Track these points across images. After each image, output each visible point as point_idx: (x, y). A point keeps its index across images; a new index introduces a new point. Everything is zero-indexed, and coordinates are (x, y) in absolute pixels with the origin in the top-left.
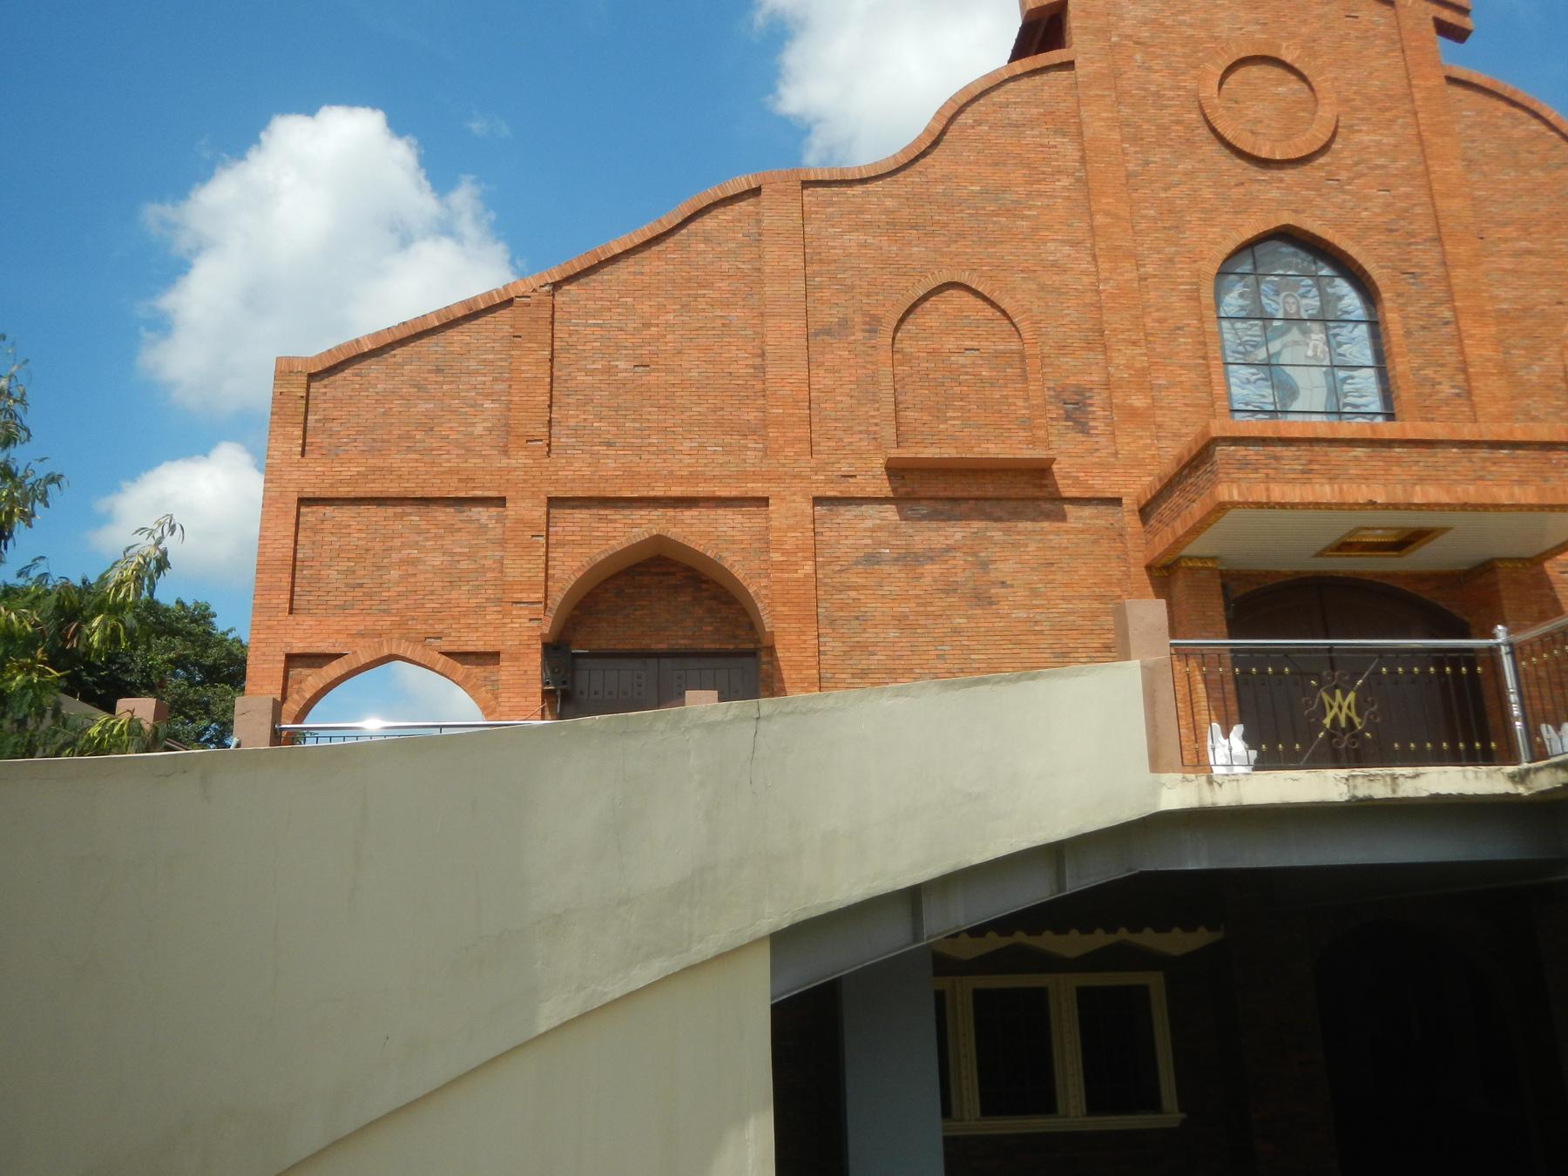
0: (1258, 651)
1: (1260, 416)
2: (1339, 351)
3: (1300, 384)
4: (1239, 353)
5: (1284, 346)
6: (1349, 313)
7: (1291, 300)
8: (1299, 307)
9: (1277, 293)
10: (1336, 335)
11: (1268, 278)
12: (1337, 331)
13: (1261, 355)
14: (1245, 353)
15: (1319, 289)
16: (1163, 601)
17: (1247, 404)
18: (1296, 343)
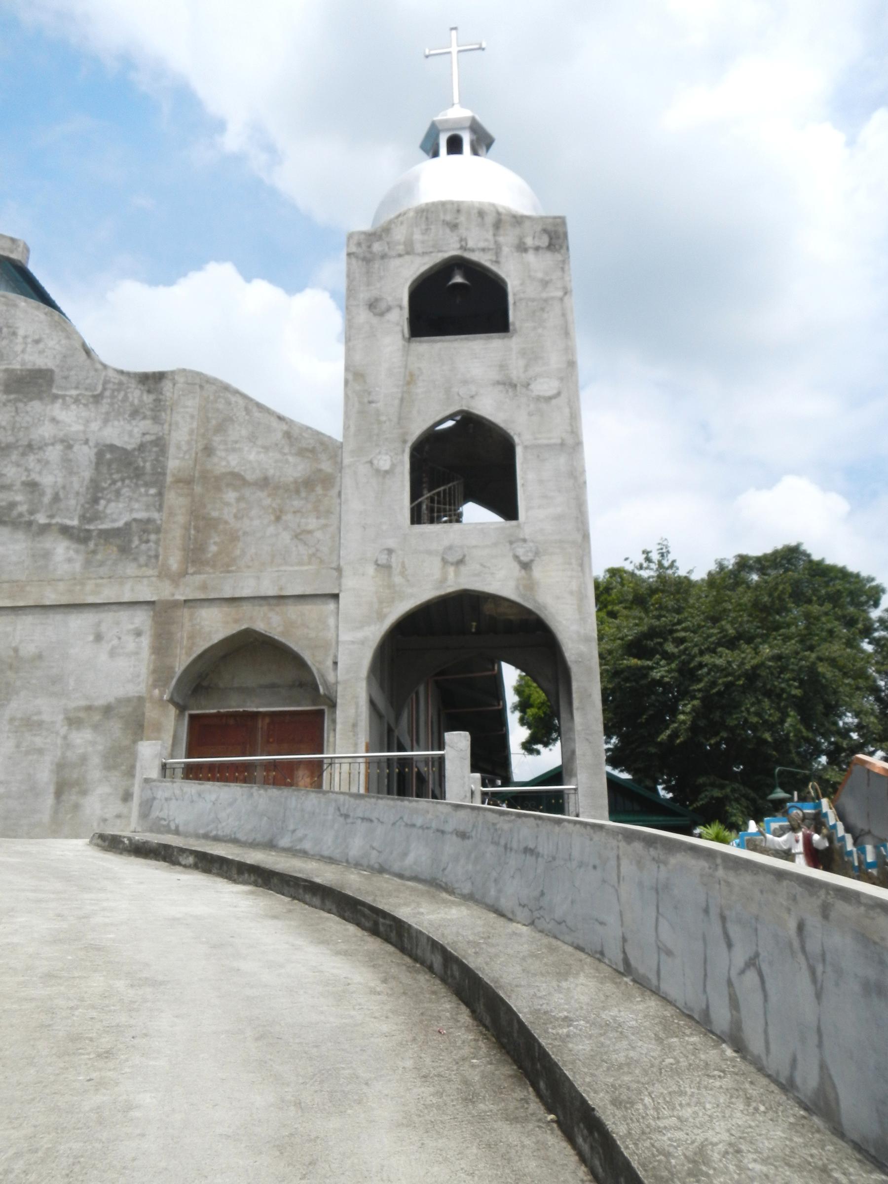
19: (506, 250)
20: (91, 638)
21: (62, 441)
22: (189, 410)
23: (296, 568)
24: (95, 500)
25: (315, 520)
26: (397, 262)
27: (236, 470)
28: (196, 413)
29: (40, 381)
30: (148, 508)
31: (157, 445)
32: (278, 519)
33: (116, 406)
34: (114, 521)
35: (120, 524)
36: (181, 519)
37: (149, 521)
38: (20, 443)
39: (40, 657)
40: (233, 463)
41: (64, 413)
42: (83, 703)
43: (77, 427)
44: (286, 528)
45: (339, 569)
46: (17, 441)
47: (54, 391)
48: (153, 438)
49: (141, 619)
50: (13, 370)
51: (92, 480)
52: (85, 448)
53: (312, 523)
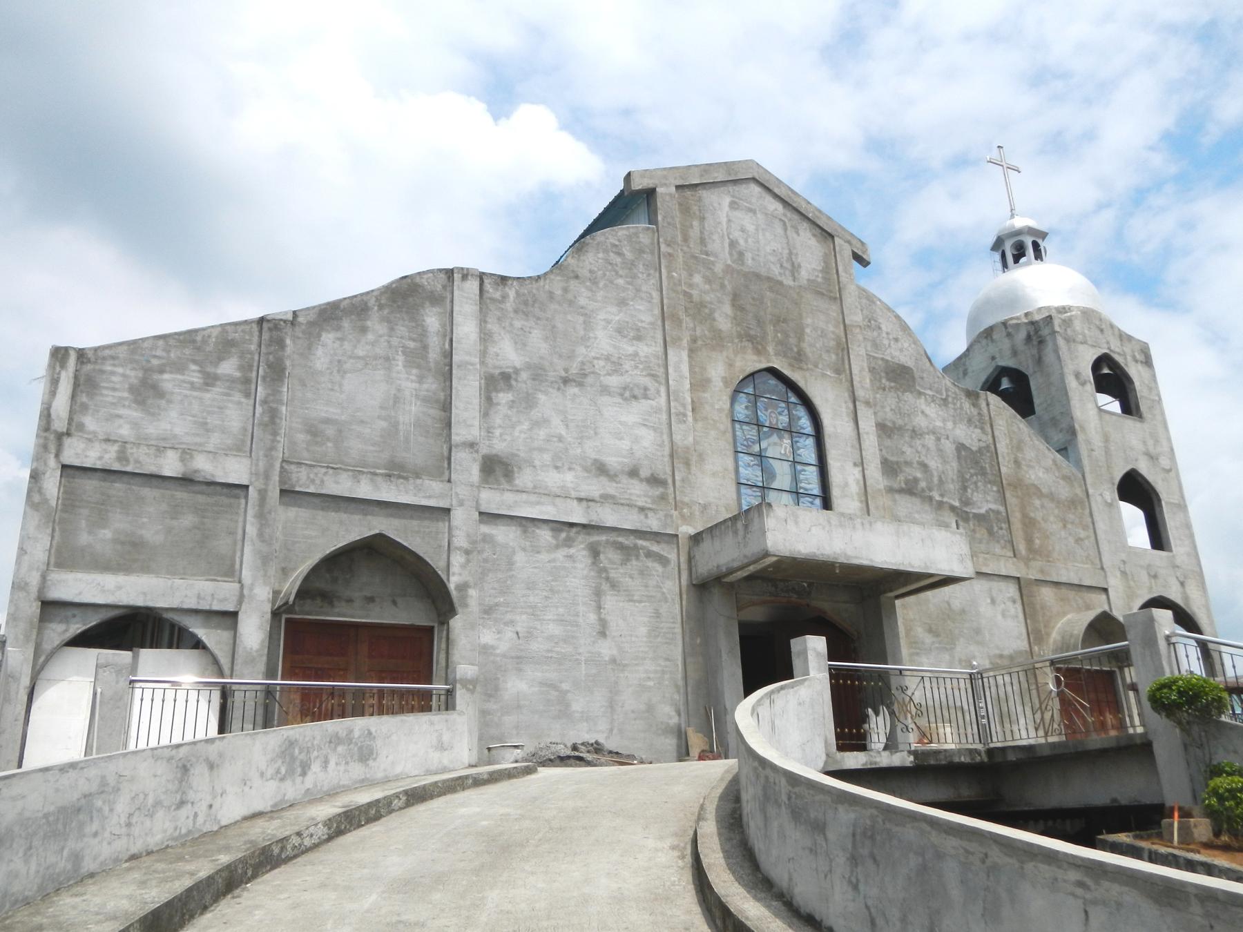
0: (851, 670)
1: (755, 489)
2: (799, 452)
3: (777, 472)
4: (744, 446)
5: (769, 445)
6: (804, 429)
7: (774, 415)
8: (777, 420)
9: (766, 410)
10: (797, 442)
11: (762, 399)
12: (797, 439)
13: (756, 449)
14: (748, 446)
15: (788, 411)
16: (824, 638)
17: (748, 480)
18: (775, 444)
19: (1129, 358)
20: (989, 601)
21: (934, 433)
22: (1002, 428)
23: (1082, 565)
24: (965, 488)
25: (1081, 531)
26: (1081, 348)
27: (1036, 483)
28: (1006, 432)
29: (907, 376)
30: (995, 503)
31: (988, 451)
32: (1065, 526)
33: (958, 411)
34: (979, 508)
35: (983, 511)
36: (1018, 515)
37: (998, 512)
38: (907, 427)
39: (963, 611)
40: (1033, 477)
41: (928, 408)
42: (997, 652)
43: (939, 424)
44: (1070, 534)
45: (1102, 568)
46: (906, 425)
47: (918, 388)
48: (984, 445)
49: (1011, 590)
50: (887, 361)
51: (959, 471)
52: (947, 442)
53: (1083, 534)
